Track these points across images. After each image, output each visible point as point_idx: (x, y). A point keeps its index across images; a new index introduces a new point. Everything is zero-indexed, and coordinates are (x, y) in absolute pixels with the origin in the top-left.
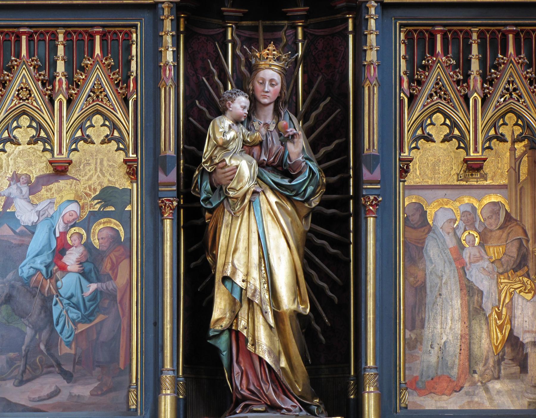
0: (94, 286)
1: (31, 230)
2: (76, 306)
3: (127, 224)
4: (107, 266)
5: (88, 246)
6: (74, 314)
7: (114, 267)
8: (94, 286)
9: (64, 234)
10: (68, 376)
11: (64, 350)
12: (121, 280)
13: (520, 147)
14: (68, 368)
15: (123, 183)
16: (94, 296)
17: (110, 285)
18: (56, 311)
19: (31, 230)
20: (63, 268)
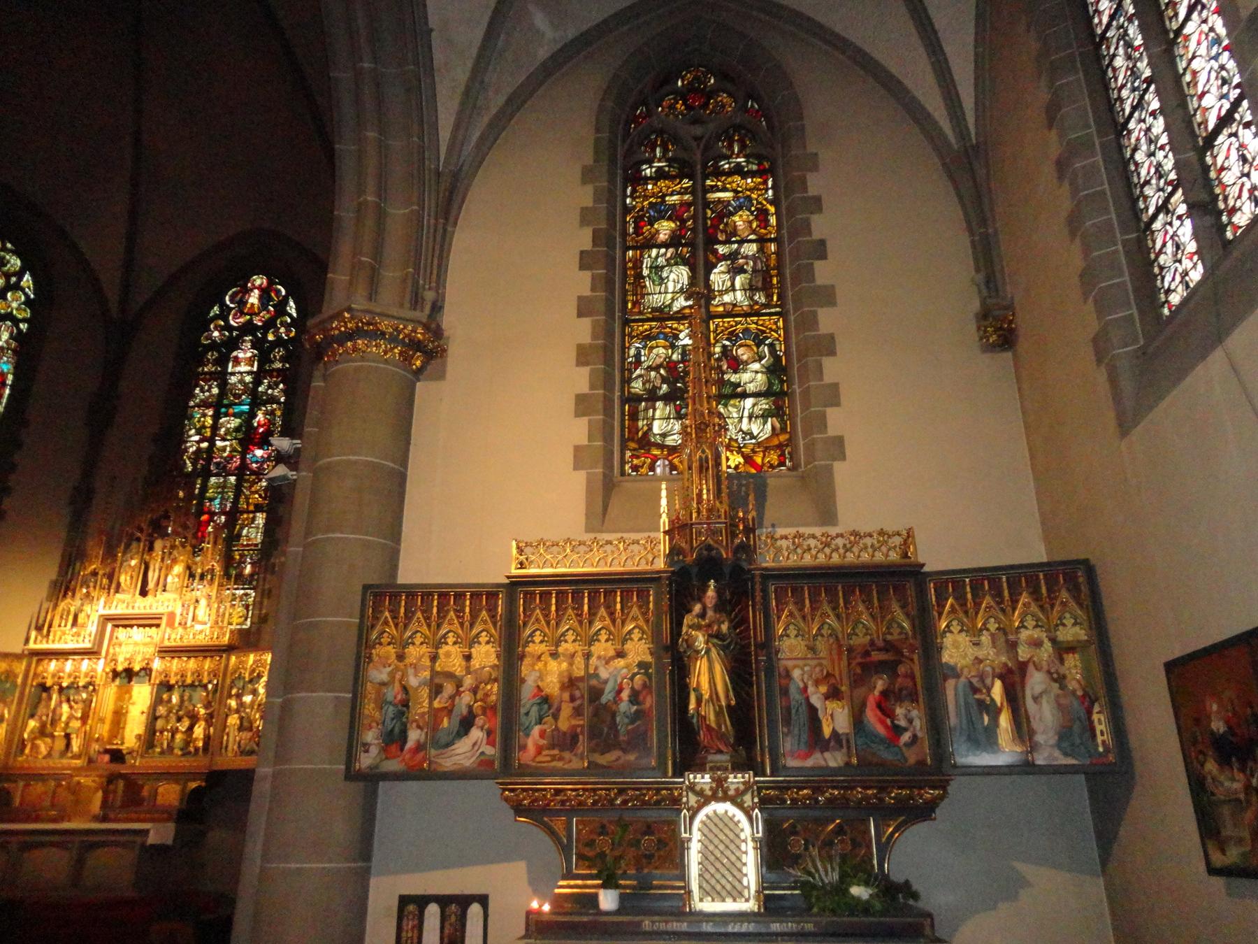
0: (635, 707)
1: (606, 682)
2: (627, 717)
3: (650, 679)
4: (641, 698)
5: (632, 688)
6: (626, 721)
7: (644, 698)
8: (635, 707)
9: (622, 683)
10: (625, 751)
11: (622, 738)
12: (648, 704)
13: (831, 641)
14: (623, 746)
15: (649, 659)
16: (637, 712)
17: (643, 707)
18: (618, 719)
19: (606, 682)
20: (621, 700)
